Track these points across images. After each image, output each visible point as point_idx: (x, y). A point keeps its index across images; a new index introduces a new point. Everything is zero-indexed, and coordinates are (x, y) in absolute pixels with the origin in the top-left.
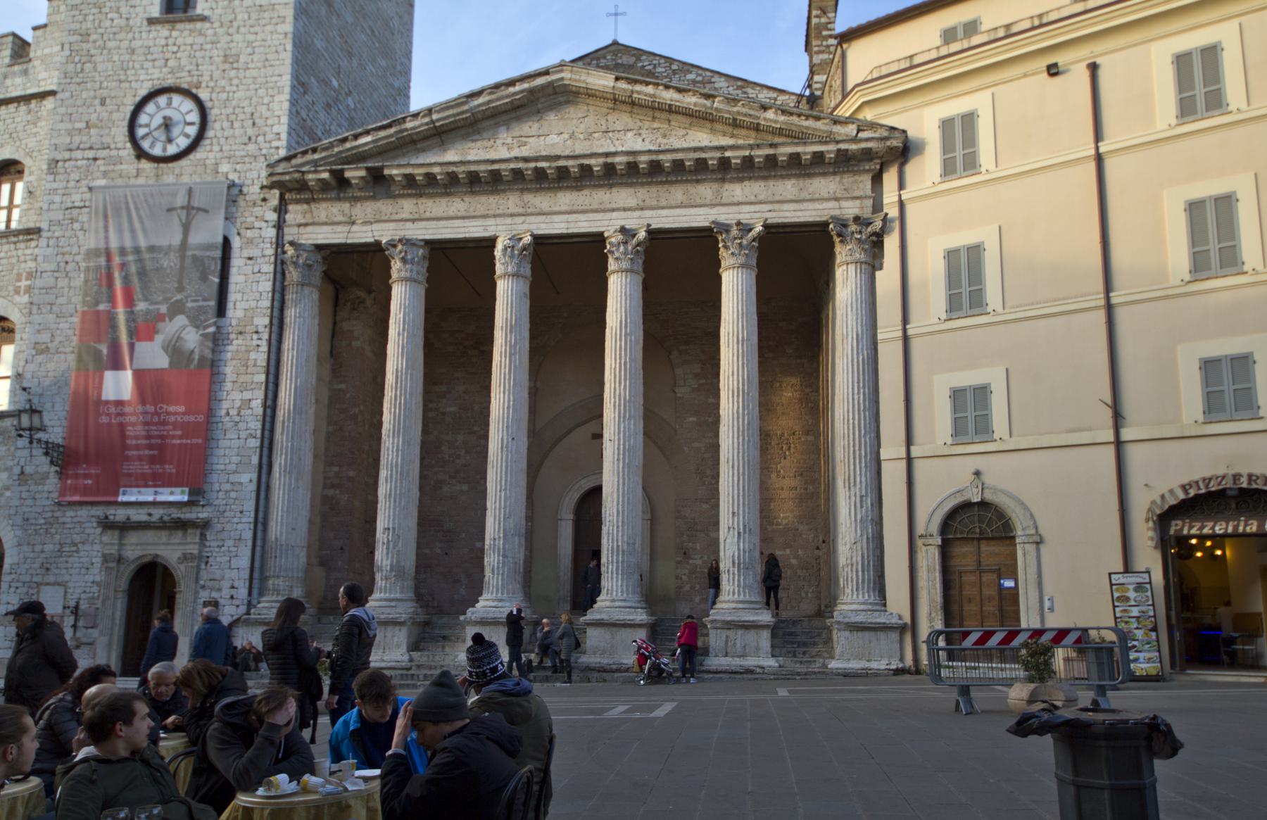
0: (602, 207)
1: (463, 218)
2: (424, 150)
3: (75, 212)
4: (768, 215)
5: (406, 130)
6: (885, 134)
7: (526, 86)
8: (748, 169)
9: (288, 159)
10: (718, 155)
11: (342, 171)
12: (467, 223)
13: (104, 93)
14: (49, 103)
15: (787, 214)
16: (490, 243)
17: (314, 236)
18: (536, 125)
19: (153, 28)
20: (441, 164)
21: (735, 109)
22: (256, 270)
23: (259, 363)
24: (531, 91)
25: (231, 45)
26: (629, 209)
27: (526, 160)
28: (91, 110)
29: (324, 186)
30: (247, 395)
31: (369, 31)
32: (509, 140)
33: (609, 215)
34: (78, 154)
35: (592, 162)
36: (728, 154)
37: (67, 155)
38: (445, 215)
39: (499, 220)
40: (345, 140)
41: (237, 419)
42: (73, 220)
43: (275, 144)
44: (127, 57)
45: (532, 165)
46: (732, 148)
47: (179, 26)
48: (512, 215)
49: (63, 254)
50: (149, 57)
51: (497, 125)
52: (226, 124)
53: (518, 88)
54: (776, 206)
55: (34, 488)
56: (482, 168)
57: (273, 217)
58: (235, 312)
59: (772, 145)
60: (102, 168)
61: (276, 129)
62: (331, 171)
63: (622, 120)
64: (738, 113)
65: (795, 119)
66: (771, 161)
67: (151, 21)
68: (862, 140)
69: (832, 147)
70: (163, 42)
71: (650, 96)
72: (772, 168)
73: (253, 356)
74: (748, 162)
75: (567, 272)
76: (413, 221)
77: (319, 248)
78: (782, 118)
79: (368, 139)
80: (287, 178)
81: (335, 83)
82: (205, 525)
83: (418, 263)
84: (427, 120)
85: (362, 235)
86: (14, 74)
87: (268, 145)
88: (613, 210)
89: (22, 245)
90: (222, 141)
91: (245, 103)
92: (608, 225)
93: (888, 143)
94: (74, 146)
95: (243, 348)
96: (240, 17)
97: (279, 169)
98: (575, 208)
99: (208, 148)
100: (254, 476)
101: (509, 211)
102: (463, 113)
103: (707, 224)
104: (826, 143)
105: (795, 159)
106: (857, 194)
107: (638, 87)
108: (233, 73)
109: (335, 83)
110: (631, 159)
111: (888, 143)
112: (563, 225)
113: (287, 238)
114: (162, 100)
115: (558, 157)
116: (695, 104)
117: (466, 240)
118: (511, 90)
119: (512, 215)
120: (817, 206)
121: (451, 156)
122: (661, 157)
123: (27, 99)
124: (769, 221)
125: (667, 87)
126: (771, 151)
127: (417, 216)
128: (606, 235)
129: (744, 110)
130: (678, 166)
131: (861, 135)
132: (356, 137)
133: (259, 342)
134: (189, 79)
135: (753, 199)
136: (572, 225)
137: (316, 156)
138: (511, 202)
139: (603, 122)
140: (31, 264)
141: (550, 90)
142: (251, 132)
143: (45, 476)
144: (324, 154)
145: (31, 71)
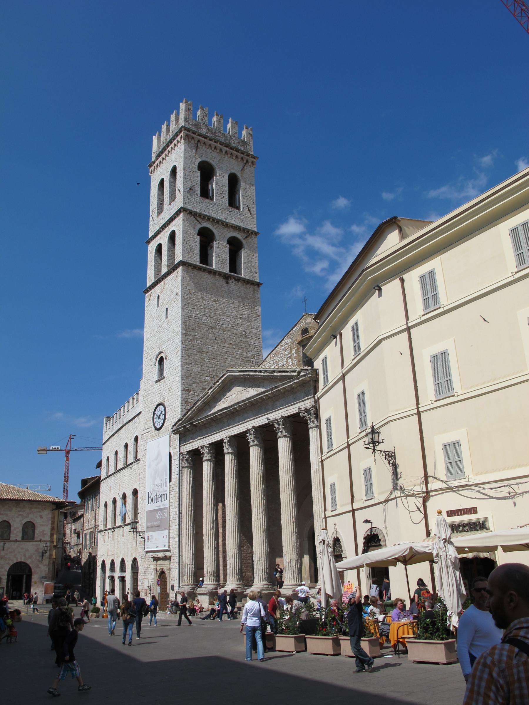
7: (220, 381)
9: (175, 425)
15: (291, 411)
16: (222, 440)
24: (222, 382)
31: (228, 345)
40: (185, 414)
59: (276, 387)
67: (156, 382)
70: (158, 388)
77: (189, 452)
83: (208, 453)
97: (174, 429)
100: (178, 539)
109: (208, 378)
112: (237, 430)
114: (158, 408)
118: (218, 383)
121: (213, 411)
132: (187, 412)
137: (180, 422)
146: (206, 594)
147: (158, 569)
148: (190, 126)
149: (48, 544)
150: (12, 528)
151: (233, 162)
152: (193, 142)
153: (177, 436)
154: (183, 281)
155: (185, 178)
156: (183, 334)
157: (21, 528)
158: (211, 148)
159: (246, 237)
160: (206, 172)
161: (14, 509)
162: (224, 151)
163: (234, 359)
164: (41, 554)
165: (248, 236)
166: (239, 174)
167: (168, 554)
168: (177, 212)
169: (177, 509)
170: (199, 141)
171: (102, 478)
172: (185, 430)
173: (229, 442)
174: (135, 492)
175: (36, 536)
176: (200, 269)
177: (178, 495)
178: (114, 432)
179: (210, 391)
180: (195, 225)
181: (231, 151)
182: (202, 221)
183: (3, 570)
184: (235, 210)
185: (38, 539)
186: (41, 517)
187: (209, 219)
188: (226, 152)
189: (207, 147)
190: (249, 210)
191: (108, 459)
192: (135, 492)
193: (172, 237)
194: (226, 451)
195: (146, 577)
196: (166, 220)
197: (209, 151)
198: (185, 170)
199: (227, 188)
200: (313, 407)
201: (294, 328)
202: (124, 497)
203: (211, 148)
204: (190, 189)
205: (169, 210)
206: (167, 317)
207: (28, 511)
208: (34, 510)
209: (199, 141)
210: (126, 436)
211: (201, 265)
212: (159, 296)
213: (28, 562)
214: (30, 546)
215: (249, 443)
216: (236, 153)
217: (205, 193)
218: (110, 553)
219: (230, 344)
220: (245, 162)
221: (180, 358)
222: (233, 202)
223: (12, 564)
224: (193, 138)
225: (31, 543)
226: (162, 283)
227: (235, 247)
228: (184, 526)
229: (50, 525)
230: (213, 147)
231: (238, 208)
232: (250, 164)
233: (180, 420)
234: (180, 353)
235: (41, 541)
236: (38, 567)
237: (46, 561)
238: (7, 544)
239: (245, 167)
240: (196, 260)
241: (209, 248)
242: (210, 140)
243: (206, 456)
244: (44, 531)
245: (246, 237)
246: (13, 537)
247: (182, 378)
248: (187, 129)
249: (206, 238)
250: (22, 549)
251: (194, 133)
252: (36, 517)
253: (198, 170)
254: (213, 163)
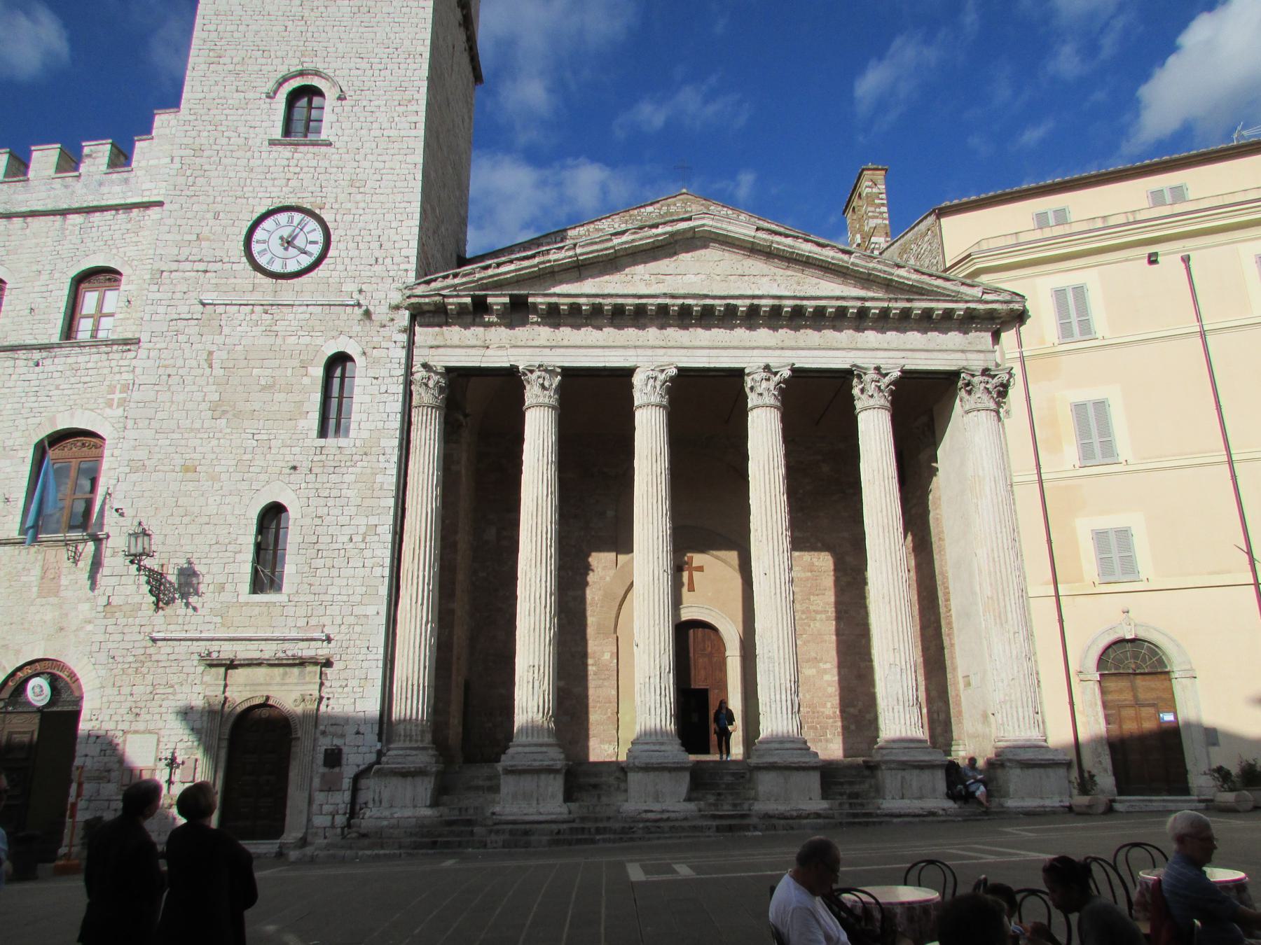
0: (742, 344)
1: (603, 347)
2: (561, 283)
3: (181, 324)
4: (902, 362)
5: (549, 261)
6: (1008, 298)
7: (668, 229)
8: (884, 321)
10: (859, 304)
11: (486, 296)
12: (607, 352)
13: (219, 207)
14: (154, 213)
16: (628, 373)
17: (447, 358)
18: (673, 265)
19: (274, 148)
20: (588, 296)
21: (871, 265)
22: (383, 390)
23: (385, 487)
24: (672, 234)
25: (358, 171)
26: (769, 348)
27: (673, 297)
28: (203, 223)
29: (462, 309)
30: (373, 520)
32: (647, 277)
33: (750, 352)
34: (188, 266)
35: (739, 302)
36: (868, 304)
37: (174, 266)
38: (584, 344)
39: (639, 351)
41: (363, 546)
42: (177, 333)
43: (403, 267)
44: (245, 175)
45: (680, 301)
46: (873, 299)
47: (301, 148)
48: (653, 347)
49: (166, 367)
50: (269, 176)
51: (635, 264)
52: (352, 245)
53: (660, 230)
54: (909, 354)
55: (122, 621)
56: (630, 301)
57: (404, 338)
60: (213, 281)
61: (404, 253)
62: (473, 297)
63: (757, 265)
64: (873, 269)
65: (925, 278)
66: (905, 314)
67: (273, 143)
68: (987, 302)
69: (962, 306)
71: (790, 247)
72: (905, 321)
73: (379, 478)
74: (885, 313)
75: (707, 407)
76: (551, 347)
77: (449, 370)
78: (915, 276)
79: (512, 267)
80: (427, 300)
84: (571, 253)
85: (496, 359)
86: (113, 182)
87: (396, 267)
88: (754, 348)
89: (118, 356)
90: (347, 261)
91: (372, 226)
92: (750, 361)
93: (1011, 306)
94: (182, 258)
95: (369, 471)
96: (367, 145)
98: (716, 344)
99: (332, 267)
101: (650, 343)
102: (607, 249)
103: (847, 366)
104: (956, 302)
105: (927, 314)
106: (979, 348)
107: (777, 238)
108: (359, 197)
110: (776, 302)
111: (1011, 306)
112: (705, 359)
115: (706, 296)
116: (833, 258)
117: (605, 369)
118: (655, 231)
119: (653, 347)
120: (945, 355)
122: (805, 303)
123: (128, 207)
124: (907, 367)
125: (807, 241)
126: (908, 305)
127: (554, 344)
128: (747, 371)
129: (879, 267)
130: (820, 313)
131: (986, 297)
133: (386, 465)
134: (313, 200)
135: (886, 346)
136: (713, 360)
137: (457, 281)
138: (652, 334)
139: (739, 266)
140: (128, 377)
141: (690, 235)
142: (377, 253)
143: (139, 607)
144: (464, 280)
145: (133, 181)
146: (556, 771)
173: (672, 379)
179: (616, 241)
195: (141, 726)
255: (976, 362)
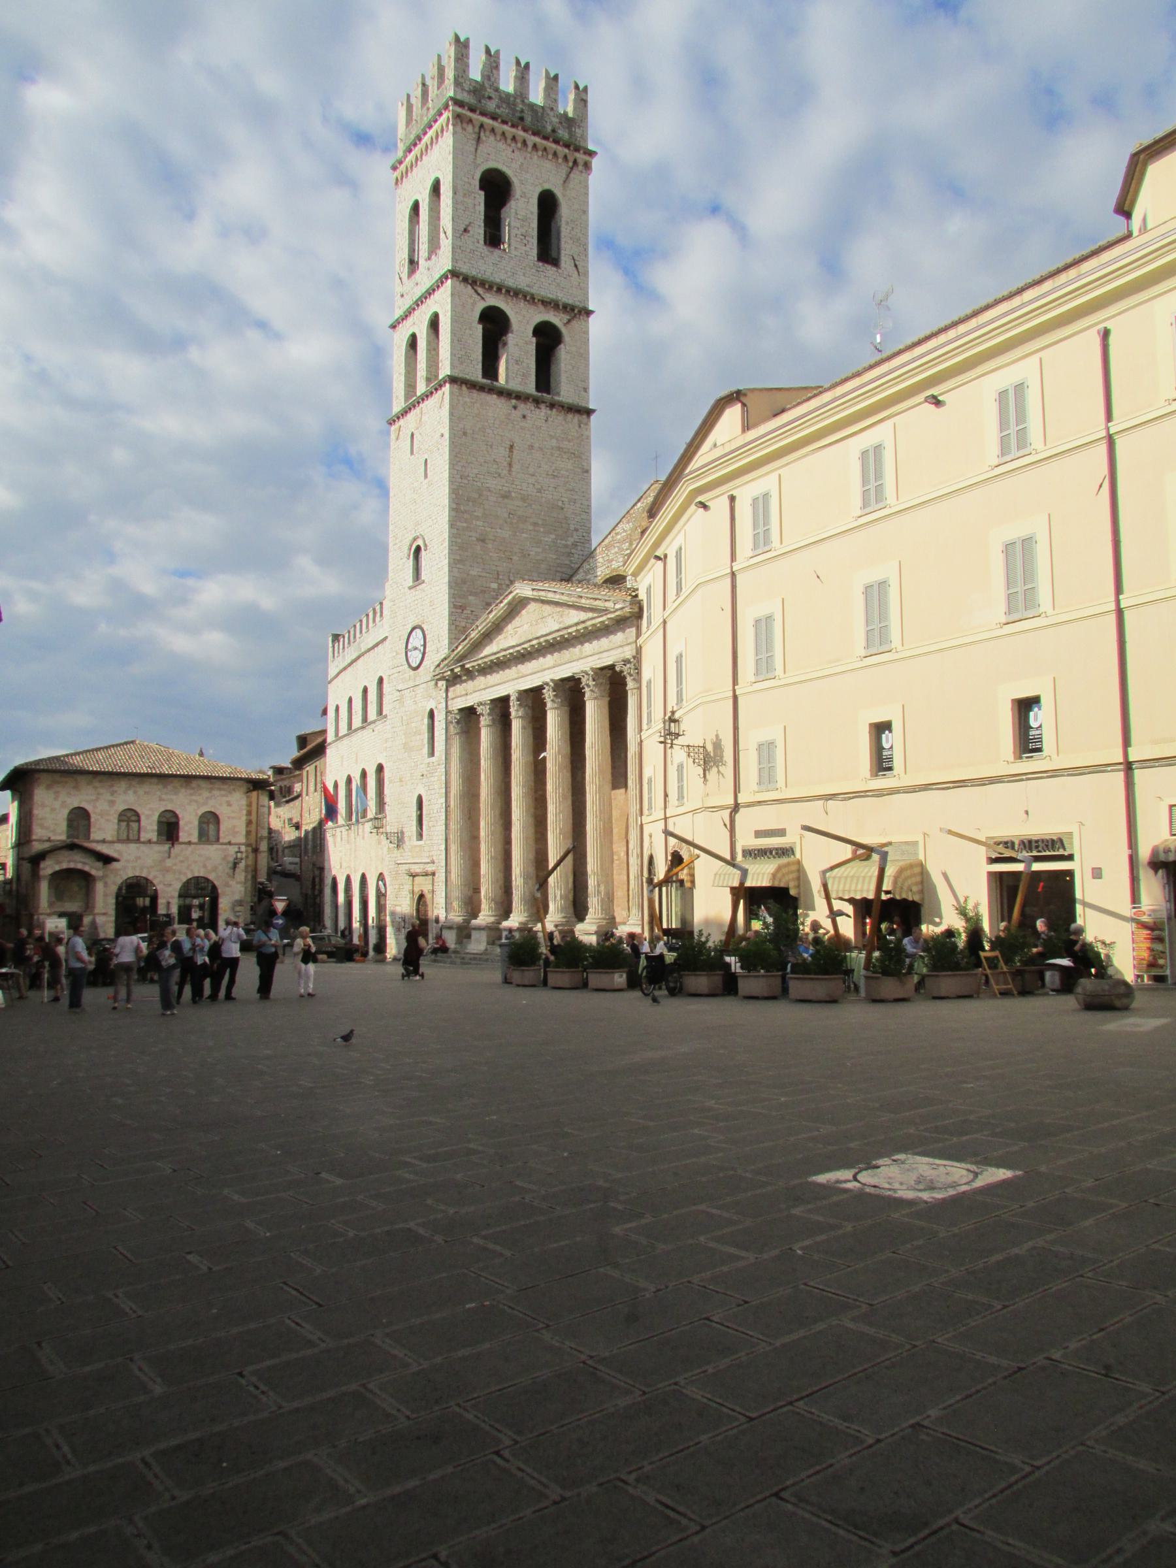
7: (506, 601)
9: (439, 665)
14: (387, 643)
24: (509, 603)
27: (505, 650)
31: (531, 528)
34: (395, 670)
58: (436, 754)
67: (410, 588)
77: (461, 710)
81: (494, 586)
82: (433, 874)
109: (494, 586)
113: (450, 708)
115: (513, 647)
147: (417, 889)
148: (465, 94)
149: (243, 848)
150: (181, 823)
151: (548, 165)
152: (470, 128)
153: (442, 684)
154: (451, 414)
155: (455, 209)
156: (451, 509)
157: (196, 823)
158: (506, 139)
159: (569, 321)
160: (496, 189)
161: (183, 790)
162: (530, 144)
163: (540, 550)
164: (231, 865)
165: (573, 318)
166: (558, 192)
167: (430, 868)
168: (441, 278)
169: (443, 800)
170: (482, 126)
171: (329, 740)
172: (455, 675)
174: (380, 769)
175: (221, 835)
176: (482, 388)
177: (443, 778)
178: (346, 664)
180: (474, 304)
181: (545, 142)
182: (487, 296)
183: (170, 889)
184: (549, 267)
185: (226, 841)
186: (229, 804)
187: (499, 289)
188: (535, 146)
189: (498, 137)
190: (576, 266)
191: (337, 708)
192: (380, 769)
193: (434, 324)
194: (513, 711)
196: (424, 290)
197: (501, 145)
198: (455, 193)
199: (535, 224)
200: (634, 657)
201: (635, 504)
202: (364, 774)
203: (506, 139)
204: (465, 230)
205: (425, 278)
206: (426, 476)
207: (206, 794)
208: (216, 793)
209: (482, 126)
210: (364, 675)
211: (485, 381)
212: (412, 435)
213: (211, 877)
214: (212, 853)
215: (545, 705)
216: (554, 146)
217: (494, 238)
218: (344, 865)
219: (535, 524)
220: (571, 164)
221: (447, 551)
222: (548, 252)
223: (185, 880)
224: (470, 121)
225: (215, 847)
226: (418, 410)
227: (547, 340)
228: (452, 826)
229: (244, 818)
230: (509, 136)
231: (555, 263)
232: (580, 168)
233: (445, 659)
234: (446, 544)
235: (230, 843)
236: (227, 885)
237: (241, 875)
238: (177, 848)
239: (572, 175)
240: (475, 373)
241: (500, 346)
242: (504, 122)
243: (484, 721)
244: (234, 827)
245: (569, 321)
246: (183, 836)
247: (450, 587)
248: (458, 103)
249: (494, 326)
250: (200, 856)
251: (472, 110)
252: (221, 805)
253: (481, 188)
254: (509, 172)
255: (628, 653)
